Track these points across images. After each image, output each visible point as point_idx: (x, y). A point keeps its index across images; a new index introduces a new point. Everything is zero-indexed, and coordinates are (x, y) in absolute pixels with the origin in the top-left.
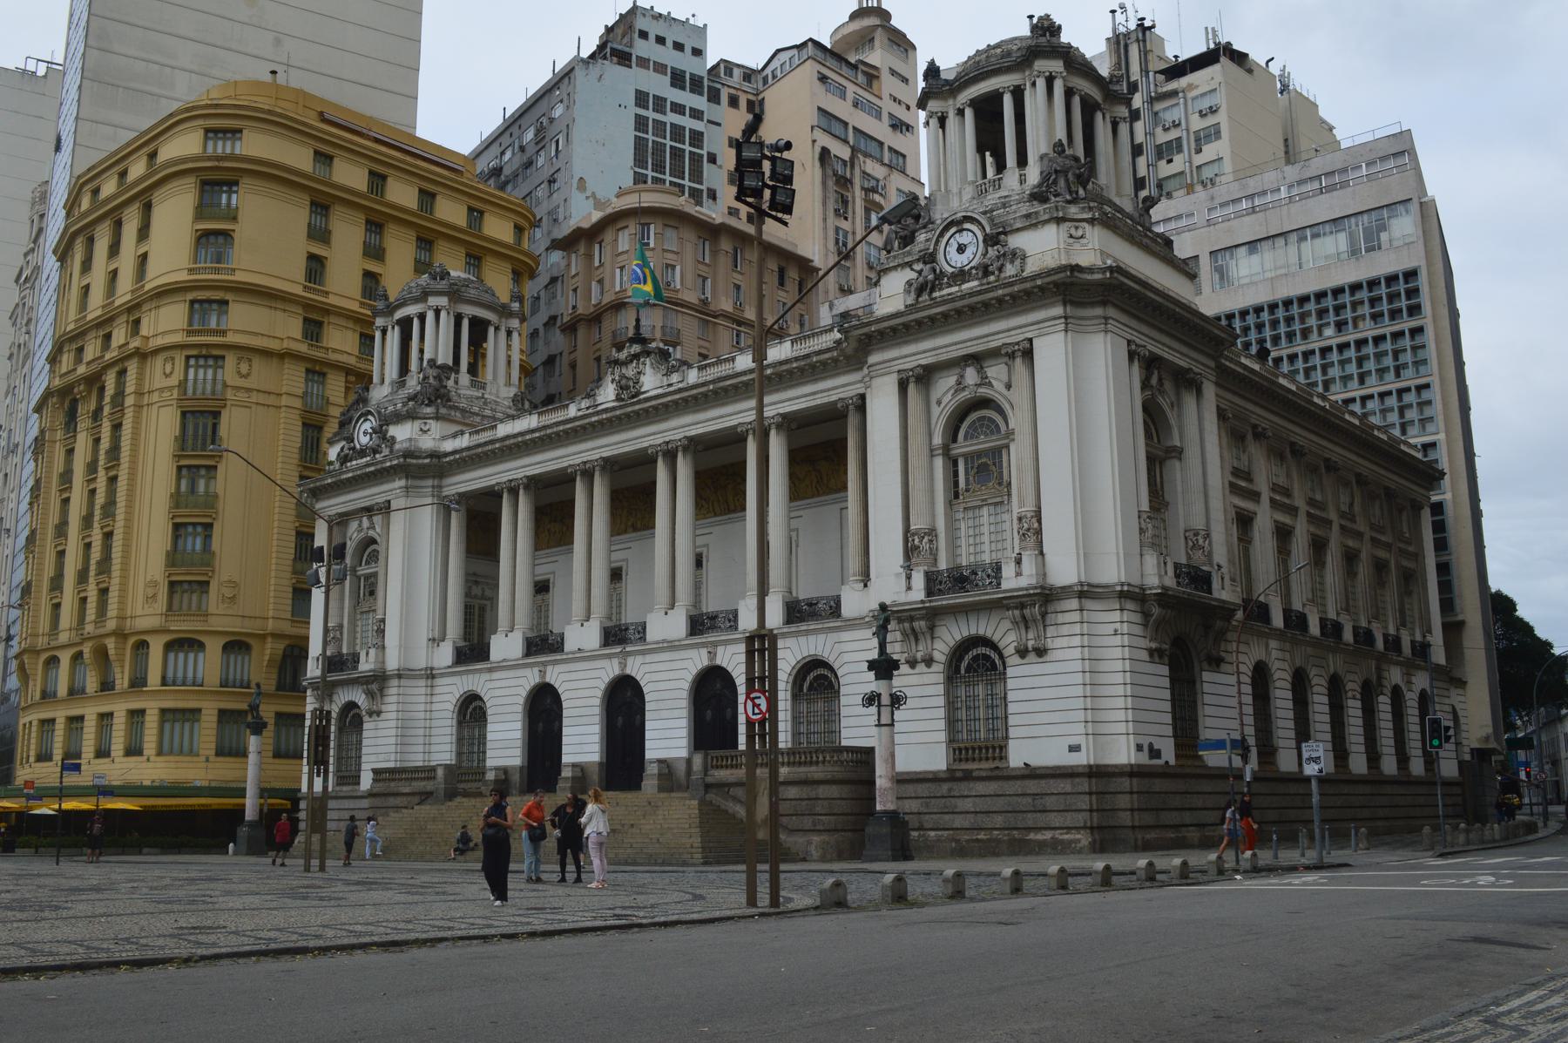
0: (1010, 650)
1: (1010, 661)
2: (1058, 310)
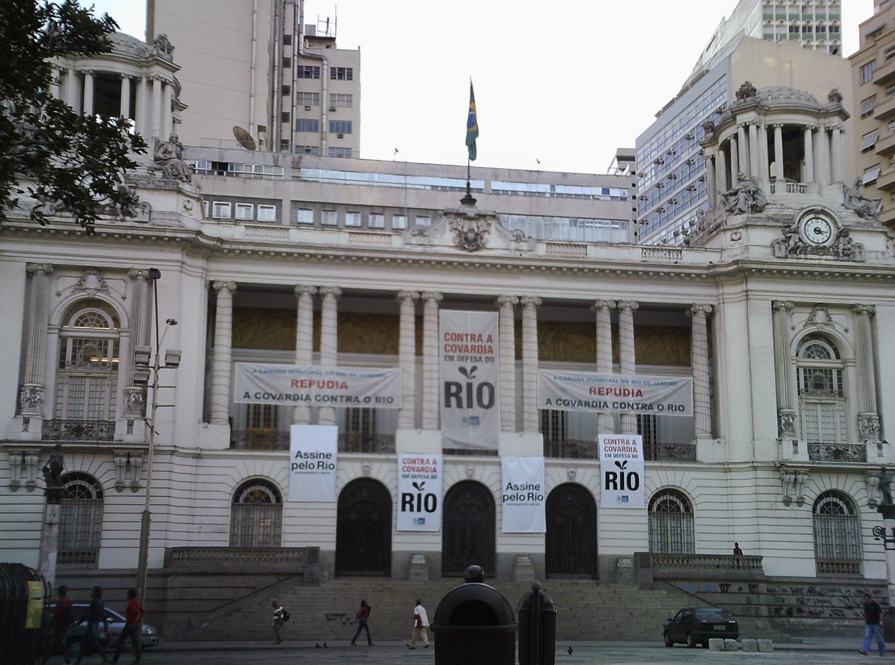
0: (112, 483)
1: (106, 493)
2: (177, 256)
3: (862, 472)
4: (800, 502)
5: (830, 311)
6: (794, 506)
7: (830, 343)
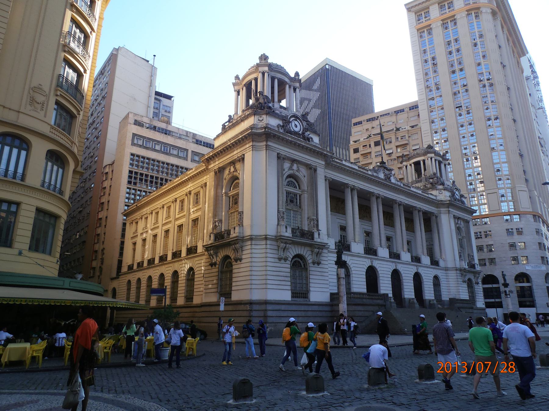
3: (311, 246)
4: (286, 259)
5: (299, 166)
6: (283, 261)
7: (297, 182)
